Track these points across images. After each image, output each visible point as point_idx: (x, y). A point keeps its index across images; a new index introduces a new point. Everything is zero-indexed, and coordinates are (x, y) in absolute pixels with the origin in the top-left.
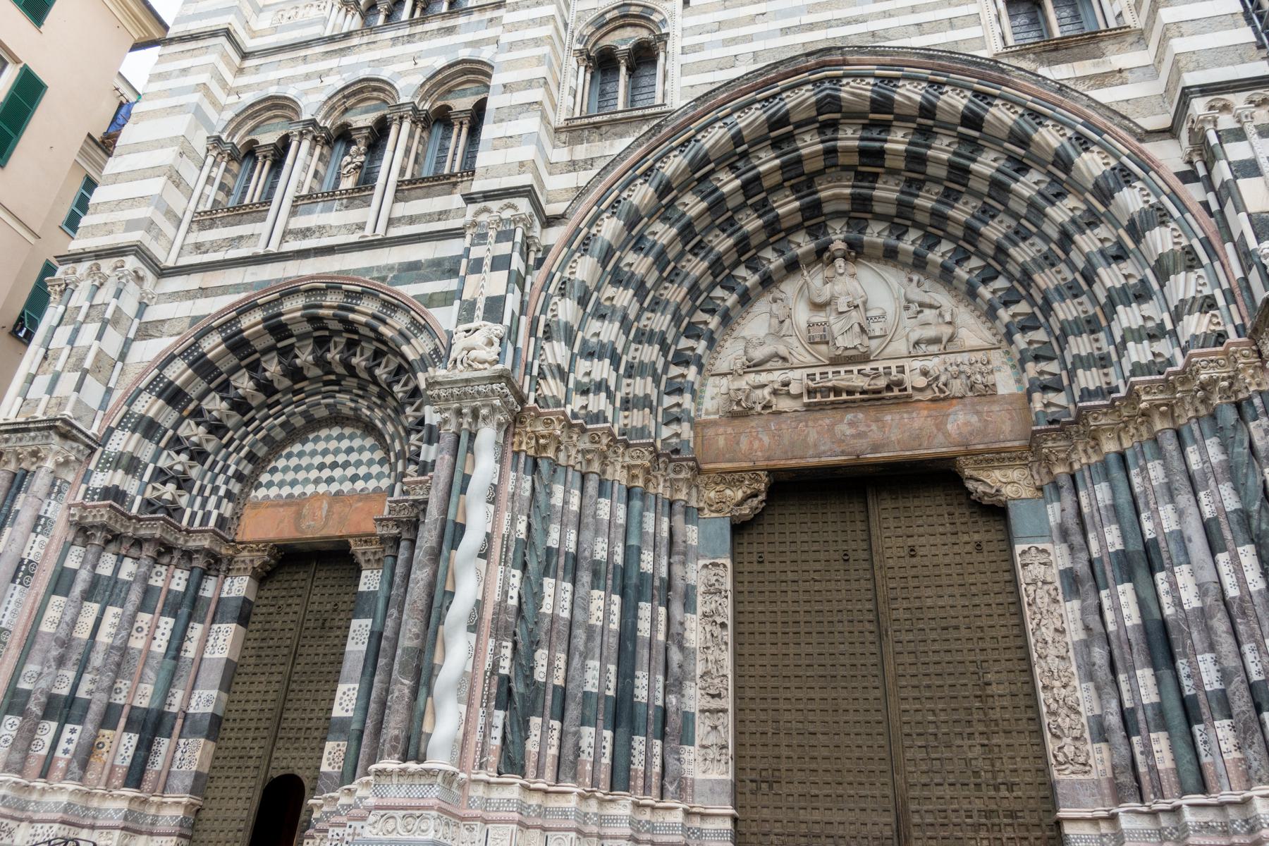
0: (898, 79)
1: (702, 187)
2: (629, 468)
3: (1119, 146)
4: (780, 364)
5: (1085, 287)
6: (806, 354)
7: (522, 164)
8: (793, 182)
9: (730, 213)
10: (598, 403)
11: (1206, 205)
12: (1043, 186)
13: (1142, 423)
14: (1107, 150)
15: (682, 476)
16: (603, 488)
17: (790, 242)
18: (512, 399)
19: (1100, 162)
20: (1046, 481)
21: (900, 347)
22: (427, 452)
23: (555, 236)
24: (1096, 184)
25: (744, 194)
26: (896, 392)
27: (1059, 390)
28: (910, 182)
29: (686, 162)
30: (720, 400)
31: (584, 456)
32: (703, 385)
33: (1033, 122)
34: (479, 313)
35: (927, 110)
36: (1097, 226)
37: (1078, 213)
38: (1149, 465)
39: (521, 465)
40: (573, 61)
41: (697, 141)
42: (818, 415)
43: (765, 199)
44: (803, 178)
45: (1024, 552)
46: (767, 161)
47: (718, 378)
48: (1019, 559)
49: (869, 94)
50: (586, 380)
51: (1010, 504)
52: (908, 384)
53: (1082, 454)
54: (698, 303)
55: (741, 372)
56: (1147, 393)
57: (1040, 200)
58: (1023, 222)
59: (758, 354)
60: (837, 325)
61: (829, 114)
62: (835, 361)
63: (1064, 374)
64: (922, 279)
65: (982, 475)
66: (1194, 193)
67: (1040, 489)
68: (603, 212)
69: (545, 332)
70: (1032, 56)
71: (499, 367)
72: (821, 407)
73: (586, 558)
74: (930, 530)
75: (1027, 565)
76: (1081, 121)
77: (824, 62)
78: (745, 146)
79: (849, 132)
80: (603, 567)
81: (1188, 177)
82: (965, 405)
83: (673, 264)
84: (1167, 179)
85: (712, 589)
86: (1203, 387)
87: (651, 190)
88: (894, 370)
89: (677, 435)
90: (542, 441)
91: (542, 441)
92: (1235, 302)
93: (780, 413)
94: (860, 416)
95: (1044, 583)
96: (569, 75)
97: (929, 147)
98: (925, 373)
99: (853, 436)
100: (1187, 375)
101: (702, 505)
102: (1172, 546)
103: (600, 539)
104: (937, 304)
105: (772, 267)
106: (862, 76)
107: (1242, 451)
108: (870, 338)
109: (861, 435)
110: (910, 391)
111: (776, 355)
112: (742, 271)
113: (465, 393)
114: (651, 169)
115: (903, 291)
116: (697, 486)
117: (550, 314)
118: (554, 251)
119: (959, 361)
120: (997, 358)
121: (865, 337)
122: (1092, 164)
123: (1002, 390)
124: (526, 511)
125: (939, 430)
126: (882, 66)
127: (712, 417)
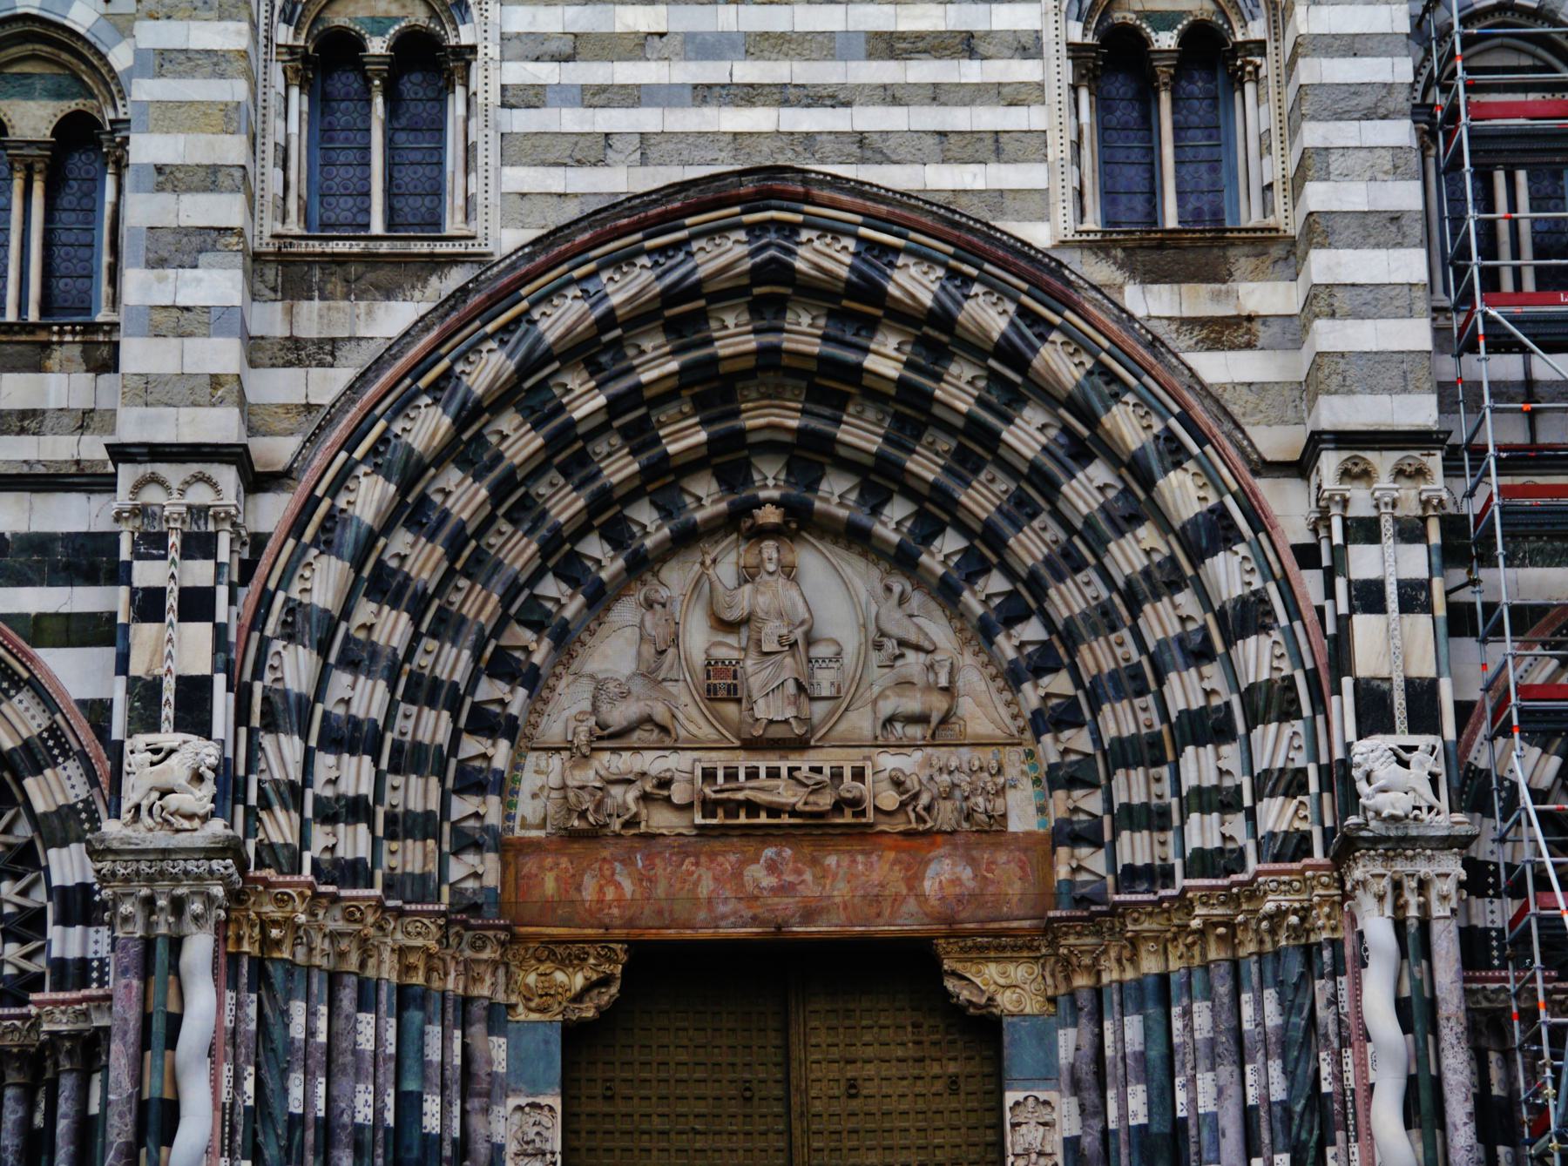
0: (897, 251)
1: (534, 402)
2: (402, 951)
3: (1225, 472)
4: (655, 735)
5: (1153, 686)
6: (702, 722)
7: (216, 381)
8: (697, 389)
9: (579, 444)
10: (354, 842)
11: (1320, 611)
12: (1111, 494)
13: (1194, 943)
14: (1210, 476)
15: (486, 955)
16: (367, 998)
17: (684, 491)
18: (236, 876)
19: (1194, 493)
20: (1062, 990)
21: (861, 722)
22: (64, 940)
23: (272, 511)
24: (1183, 528)
25: (608, 413)
26: (848, 818)
27: (1097, 843)
28: (900, 420)
29: (511, 366)
30: (551, 805)
31: (332, 943)
32: (517, 766)
33: (1106, 390)
34: (168, 712)
35: (942, 318)
36: (1180, 590)
37: (1157, 558)
38: (1195, 1007)
39: (244, 980)
40: (276, 72)
41: (534, 322)
42: (717, 845)
43: (646, 417)
44: (715, 384)
45: (1017, 1103)
46: (656, 363)
47: (543, 755)
48: (1008, 1115)
49: (844, 272)
50: (329, 792)
51: (1006, 1021)
52: (868, 804)
53: (1114, 965)
54: (513, 610)
55: (586, 750)
56: (1204, 904)
57: (1104, 526)
58: (1077, 541)
59: (619, 715)
60: (757, 675)
61: (771, 288)
62: (751, 745)
63: (1107, 820)
64: (909, 588)
65: (969, 971)
66: (1310, 584)
67: (1052, 1000)
68: (358, 463)
69: (263, 714)
70: (1119, 253)
71: (217, 826)
72: (723, 831)
73: (344, 1126)
74: (883, 1052)
75: (1019, 1124)
76: (1176, 409)
77: (767, 190)
78: (618, 332)
79: (806, 320)
80: (368, 1135)
81: (1307, 556)
82: (955, 847)
83: (473, 543)
84: (1281, 552)
85: (530, 1149)
86: (1269, 917)
87: (447, 420)
88: (847, 773)
89: (476, 875)
90: (275, 933)
91: (275, 933)
92: (1331, 791)
93: (650, 837)
94: (788, 852)
95: (1040, 1154)
96: (271, 112)
97: (938, 378)
98: (897, 784)
99: (776, 891)
100: (1252, 892)
101: (514, 999)
102: (1205, 1134)
103: (361, 1087)
104: (927, 645)
105: (649, 543)
106: (837, 233)
107: (1300, 1021)
108: (812, 699)
109: (784, 889)
110: (870, 817)
111: (648, 720)
112: (594, 547)
113: (162, 873)
114: (447, 374)
115: (874, 609)
116: (507, 965)
117: (269, 676)
118: (271, 546)
119: (954, 764)
120: (1013, 761)
121: (803, 699)
122: (1183, 493)
123: (1015, 825)
124: (253, 1058)
125: (911, 888)
126: (873, 221)
127: (534, 834)
